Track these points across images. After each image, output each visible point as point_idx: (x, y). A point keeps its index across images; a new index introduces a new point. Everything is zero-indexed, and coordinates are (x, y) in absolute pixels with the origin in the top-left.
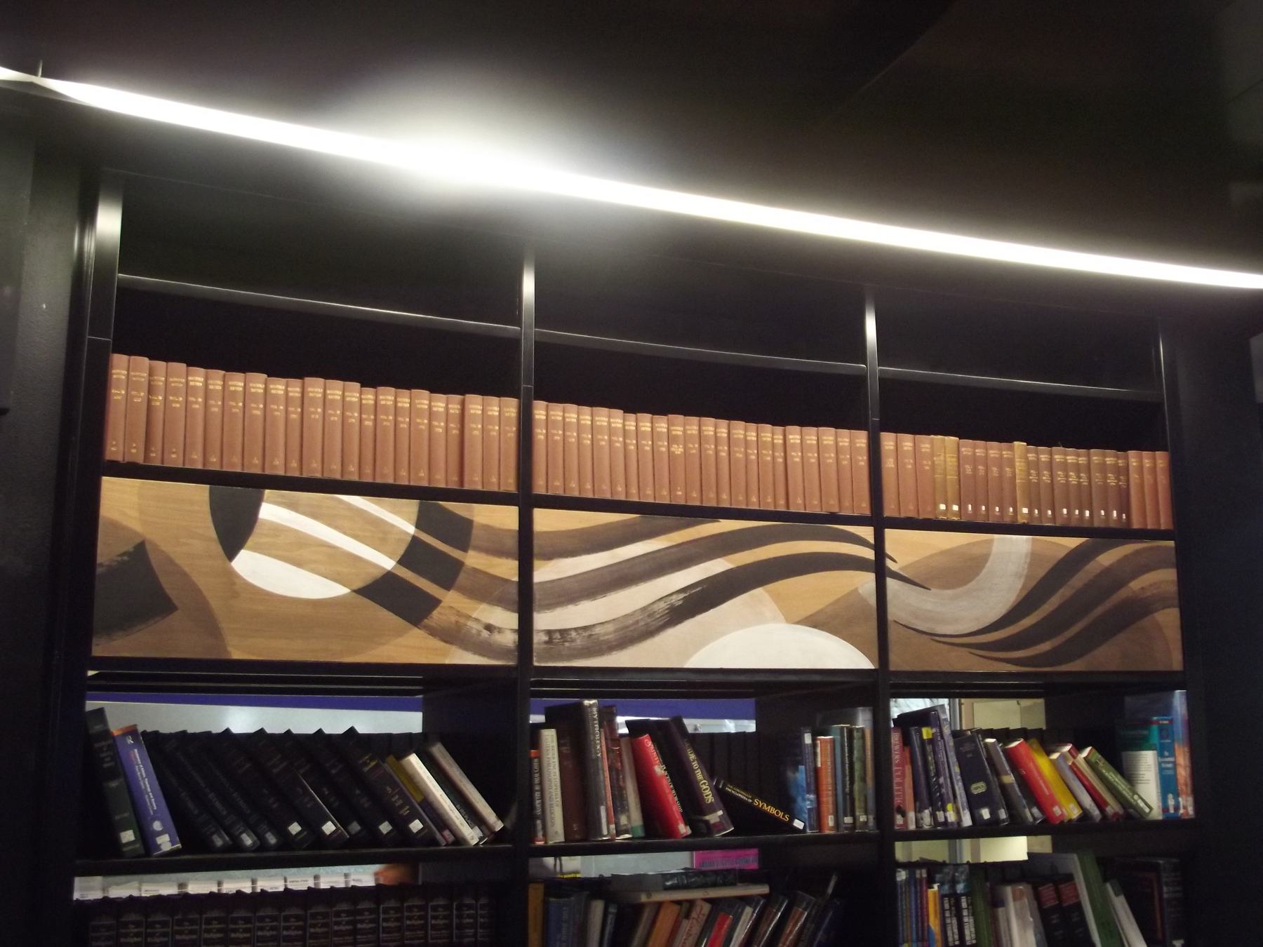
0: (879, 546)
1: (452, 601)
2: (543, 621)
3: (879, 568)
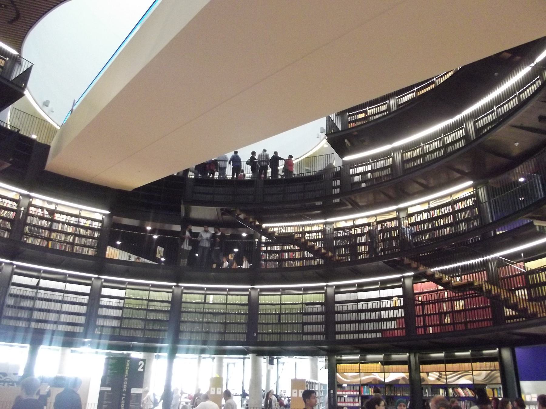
1: (442, 380)
2: (448, 380)
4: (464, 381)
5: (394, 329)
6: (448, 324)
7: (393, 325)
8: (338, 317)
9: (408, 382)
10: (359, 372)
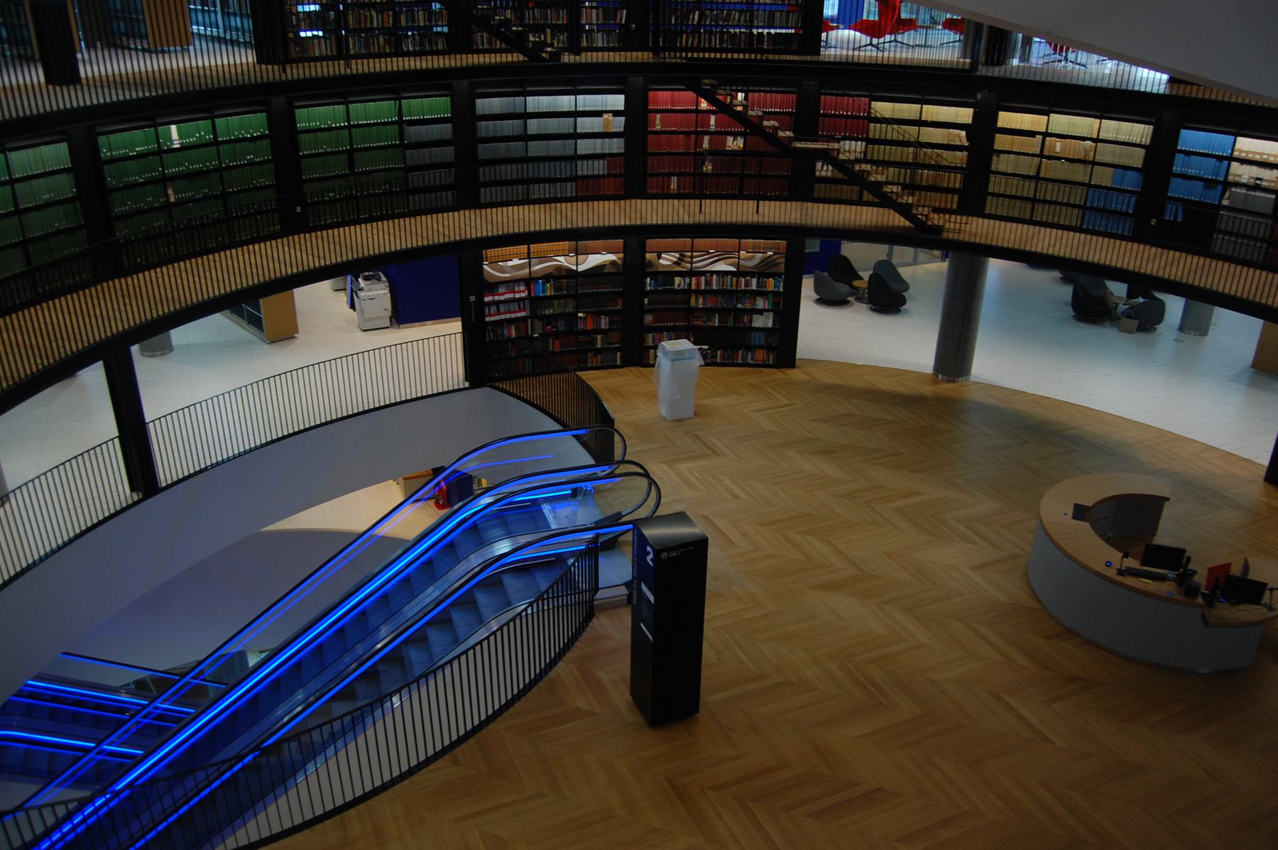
0: (739, 255)
1: (683, 264)
3: (739, 258)
4: (721, 267)
5: (603, 176)
6: (707, 175)
7: (599, 167)
8: (484, 151)
9: (621, 270)
10: (529, 257)
